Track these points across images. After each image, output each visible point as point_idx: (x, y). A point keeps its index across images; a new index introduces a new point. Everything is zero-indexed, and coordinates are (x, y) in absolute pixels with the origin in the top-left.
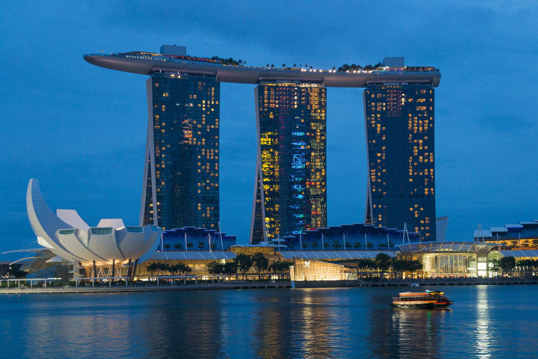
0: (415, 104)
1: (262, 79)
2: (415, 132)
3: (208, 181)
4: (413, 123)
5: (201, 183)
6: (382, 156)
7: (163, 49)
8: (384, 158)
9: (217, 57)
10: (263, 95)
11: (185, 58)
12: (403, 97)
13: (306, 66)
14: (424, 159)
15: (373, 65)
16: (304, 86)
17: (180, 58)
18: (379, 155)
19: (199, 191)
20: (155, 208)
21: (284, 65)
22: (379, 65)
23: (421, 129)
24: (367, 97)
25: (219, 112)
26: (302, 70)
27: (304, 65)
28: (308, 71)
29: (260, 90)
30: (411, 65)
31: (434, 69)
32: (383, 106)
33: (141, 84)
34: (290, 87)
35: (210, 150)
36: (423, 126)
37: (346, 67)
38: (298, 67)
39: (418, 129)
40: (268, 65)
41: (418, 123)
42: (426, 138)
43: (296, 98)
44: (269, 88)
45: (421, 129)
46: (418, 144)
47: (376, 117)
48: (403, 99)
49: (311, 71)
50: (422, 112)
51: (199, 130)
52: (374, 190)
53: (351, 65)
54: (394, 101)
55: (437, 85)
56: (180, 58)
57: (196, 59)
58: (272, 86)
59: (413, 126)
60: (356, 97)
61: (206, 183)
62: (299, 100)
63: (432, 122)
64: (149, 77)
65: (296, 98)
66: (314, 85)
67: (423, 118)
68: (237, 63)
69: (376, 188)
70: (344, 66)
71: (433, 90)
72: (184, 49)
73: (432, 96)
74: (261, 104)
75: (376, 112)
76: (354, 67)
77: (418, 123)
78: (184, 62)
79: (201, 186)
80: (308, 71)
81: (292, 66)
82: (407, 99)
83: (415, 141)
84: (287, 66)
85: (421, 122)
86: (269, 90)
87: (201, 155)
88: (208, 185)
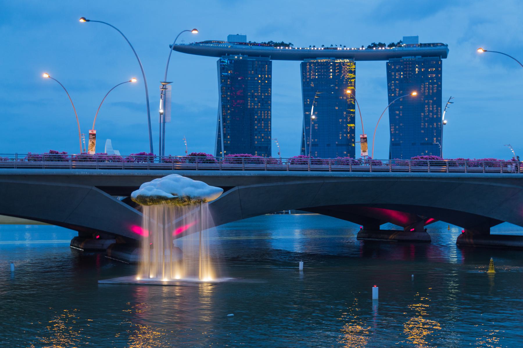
0: (426, 72)
2: (426, 94)
3: (263, 135)
4: (425, 87)
5: (258, 136)
6: (399, 113)
7: (230, 37)
8: (401, 115)
9: (271, 42)
10: (306, 69)
11: (246, 44)
12: (417, 67)
13: (341, 45)
14: (433, 116)
15: (396, 43)
16: (338, 61)
17: (241, 44)
18: (398, 112)
19: (256, 142)
20: (223, 155)
21: (323, 46)
22: (401, 42)
23: (431, 91)
24: (388, 67)
25: (271, 83)
26: (338, 49)
27: (339, 45)
28: (343, 49)
29: (303, 66)
30: (423, 42)
32: (401, 75)
33: (211, 63)
34: (326, 62)
35: (264, 111)
36: (433, 90)
37: (375, 45)
38: (334, 46)
39: (429, 92)
40: (310, 46)
41: (429, 87)
42: (435, 98)
43: (331, 70)
44: (310, 63)
45: (431, 91)
46: (428, 104)
47: (395, 85)
48: (417, 69)
49: (345, 49)
50: (432, 78)
51: (256, 97)
52: (393, 140)
53: (378, 43)
54: (410, 71)
55: (445, 56)
56: (241, 44)
57: (255, 44)
58: (313, 63)
59: (425, 90)
60: (378, 70)
61: (261, 136)
62: (334, 72)
63: (440, 86)
65: (331, 70)
67: (433, 83)
68: (288, 45)
69: (395, 139)
70: (372, 44)
71: (441, 61)
72: (245, 37)
73: (441, 66)
74: (304, 76)
75: (395, 80)
76: (381, 45)
77: (429, 87)
78: (244, 47)
79: (258, 139)
80: (343, 49)
81: (329, 46)
82: (420, 69)
83: (426, 101)
84: (326, 46)
85: (431, 86)
86: (310, 65)
87: (258, 116)
88: (263, 138)
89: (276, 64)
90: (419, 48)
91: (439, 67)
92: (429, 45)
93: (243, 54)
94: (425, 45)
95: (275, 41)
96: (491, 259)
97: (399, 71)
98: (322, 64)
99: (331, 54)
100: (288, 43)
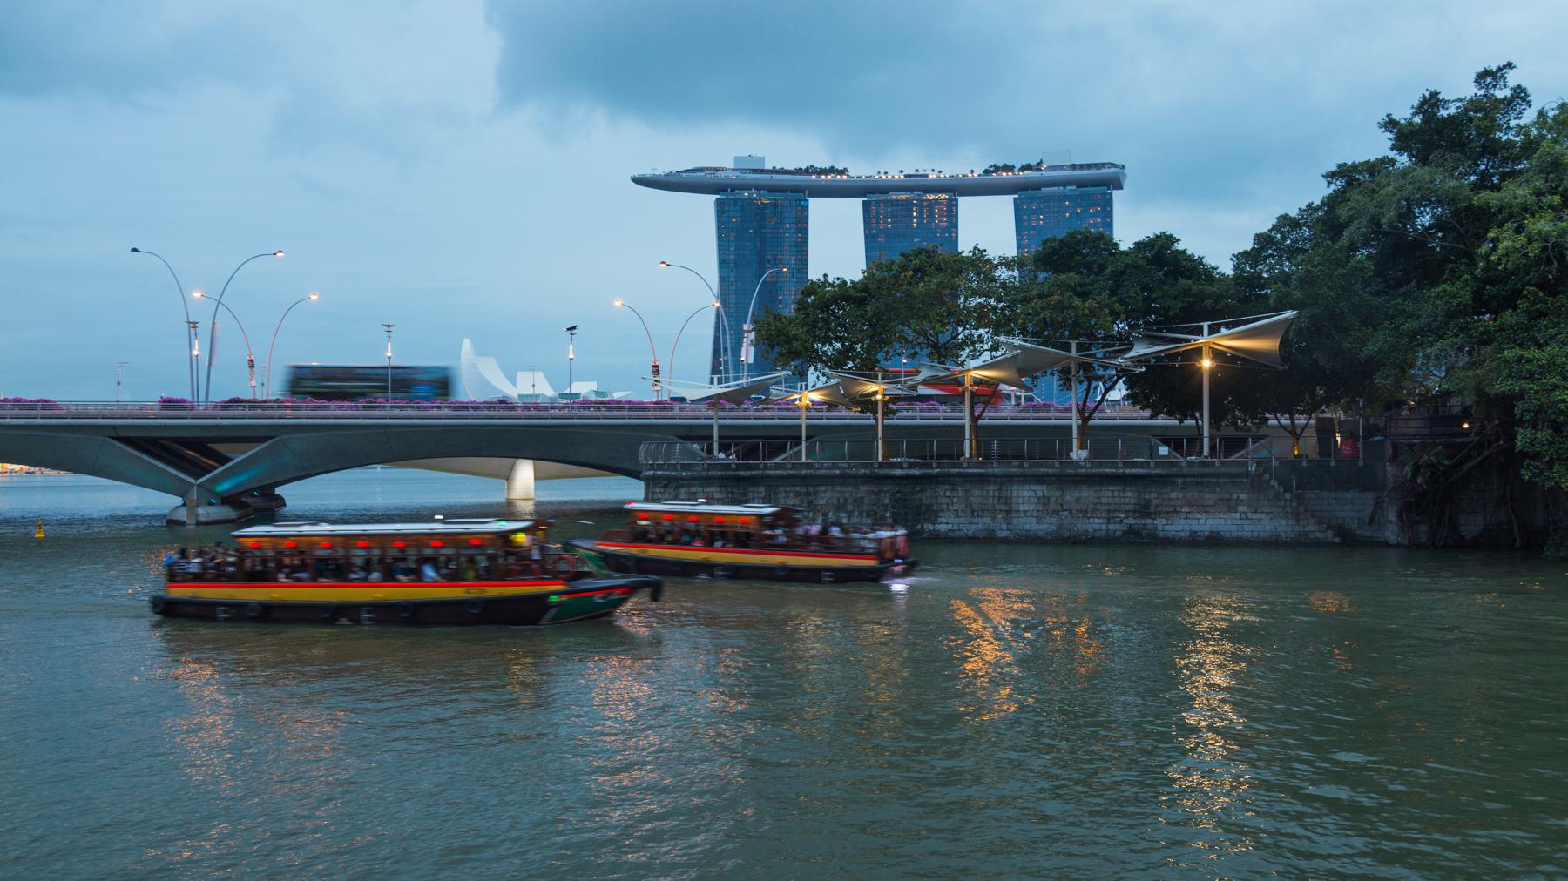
1: (871, 193)
7: (737, 159)
11: (763, 171)
15: (1033, 163)
31: (1114, 165)
56: (755, 171)
62: (920, 217)
64: (714, 197)
66: (944, 196)
68: (843, 172)
89: (816, 205)
90: (1070, 173)
91: (1108, 203)
92: (1089, 166)
93: (758, 188)
94: (1082, 167)
95: (818, 165)
96: (901, 532)
97: (1035, 213)
98: (895, 203)
99: (918, 185)
100: (840, 168)
